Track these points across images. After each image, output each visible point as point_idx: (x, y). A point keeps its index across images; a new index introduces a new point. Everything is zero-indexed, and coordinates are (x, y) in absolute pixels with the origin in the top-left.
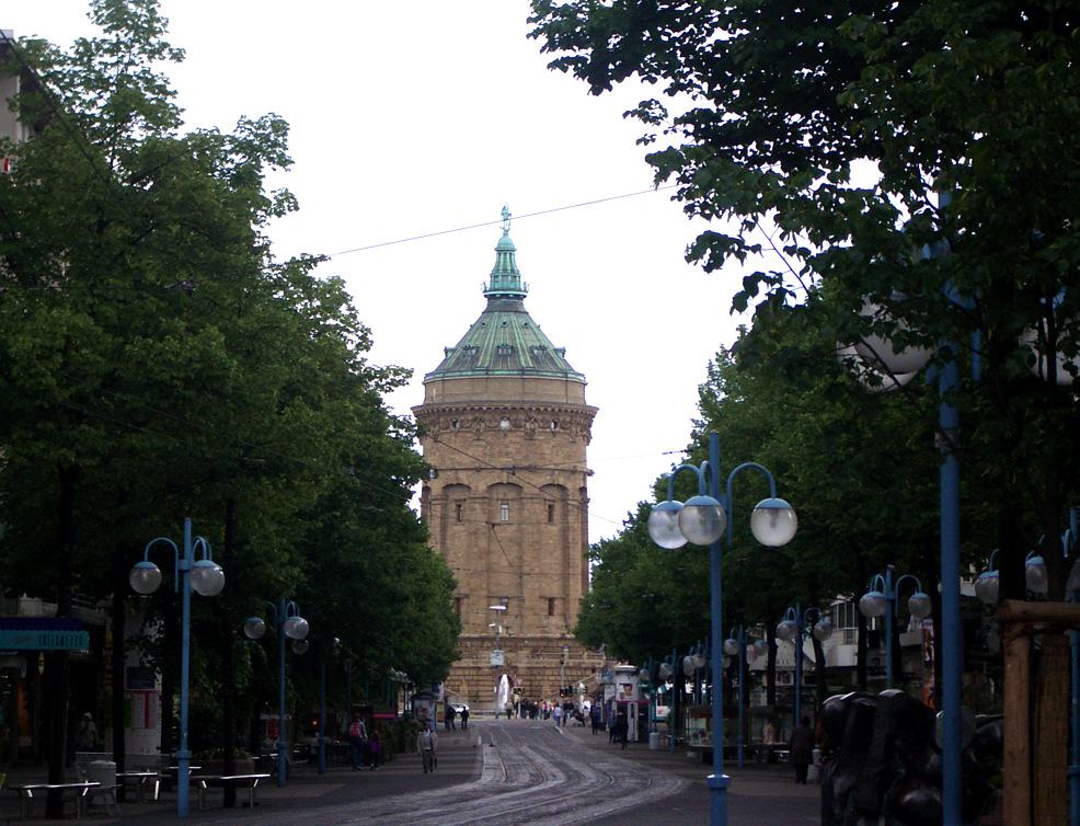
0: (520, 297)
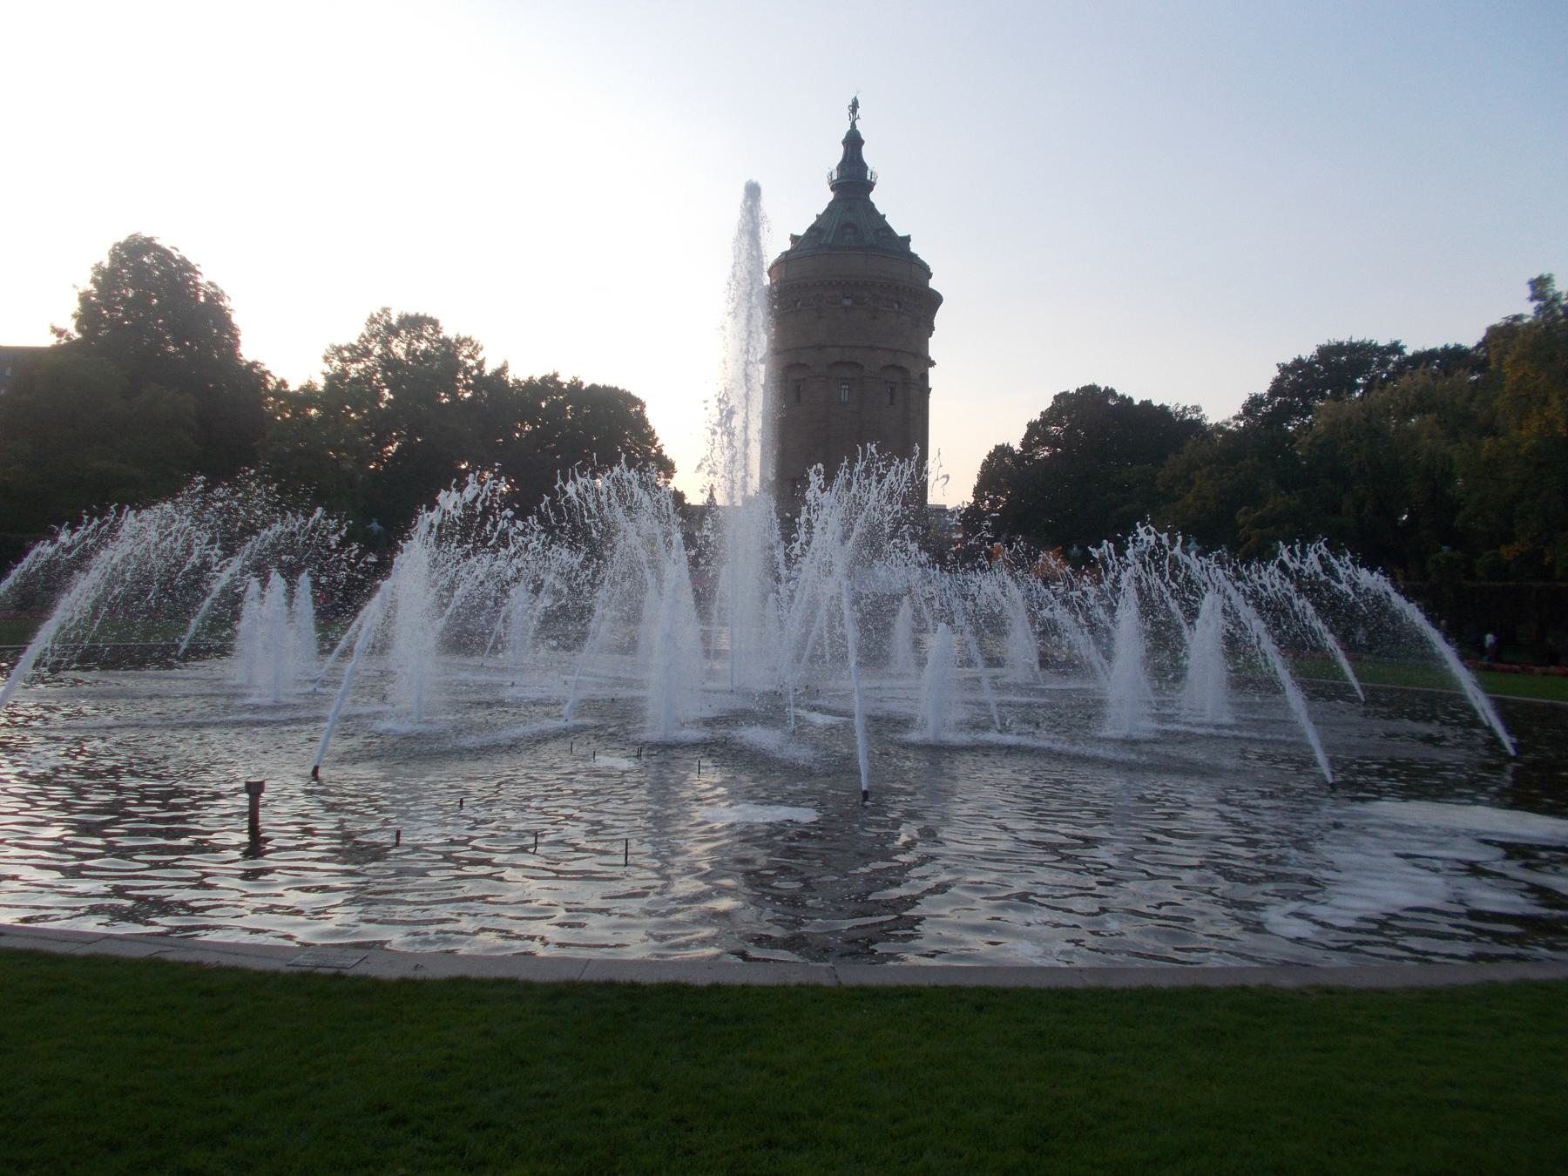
0: (870, 186)
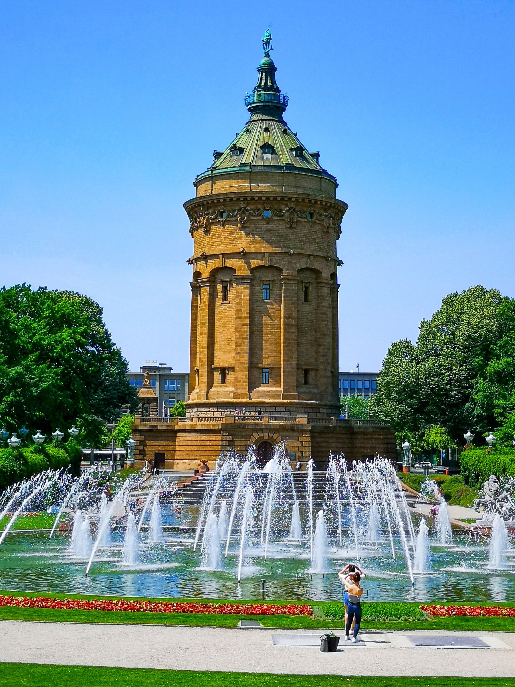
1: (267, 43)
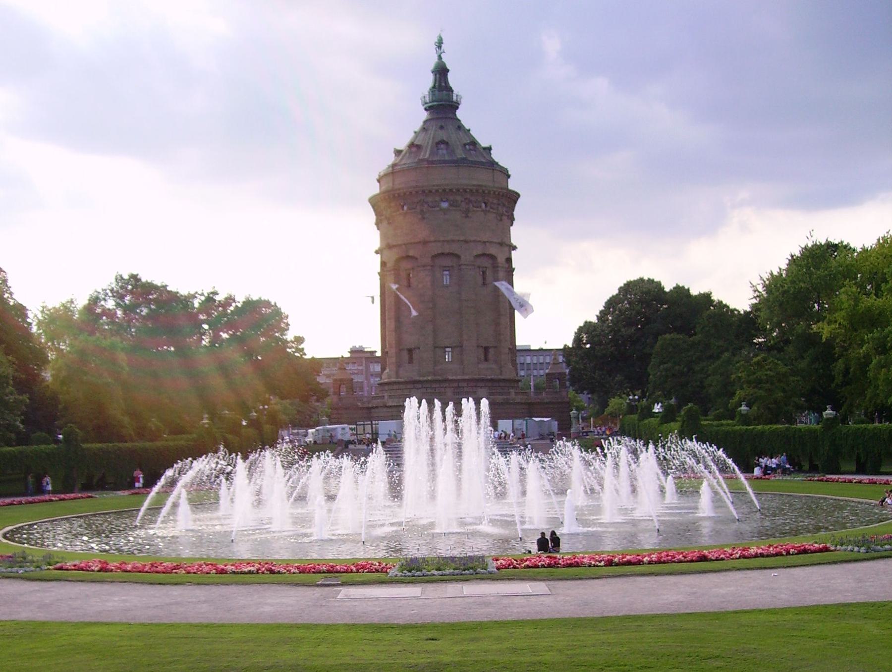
0: (455, 106)
1: (440, 47)
